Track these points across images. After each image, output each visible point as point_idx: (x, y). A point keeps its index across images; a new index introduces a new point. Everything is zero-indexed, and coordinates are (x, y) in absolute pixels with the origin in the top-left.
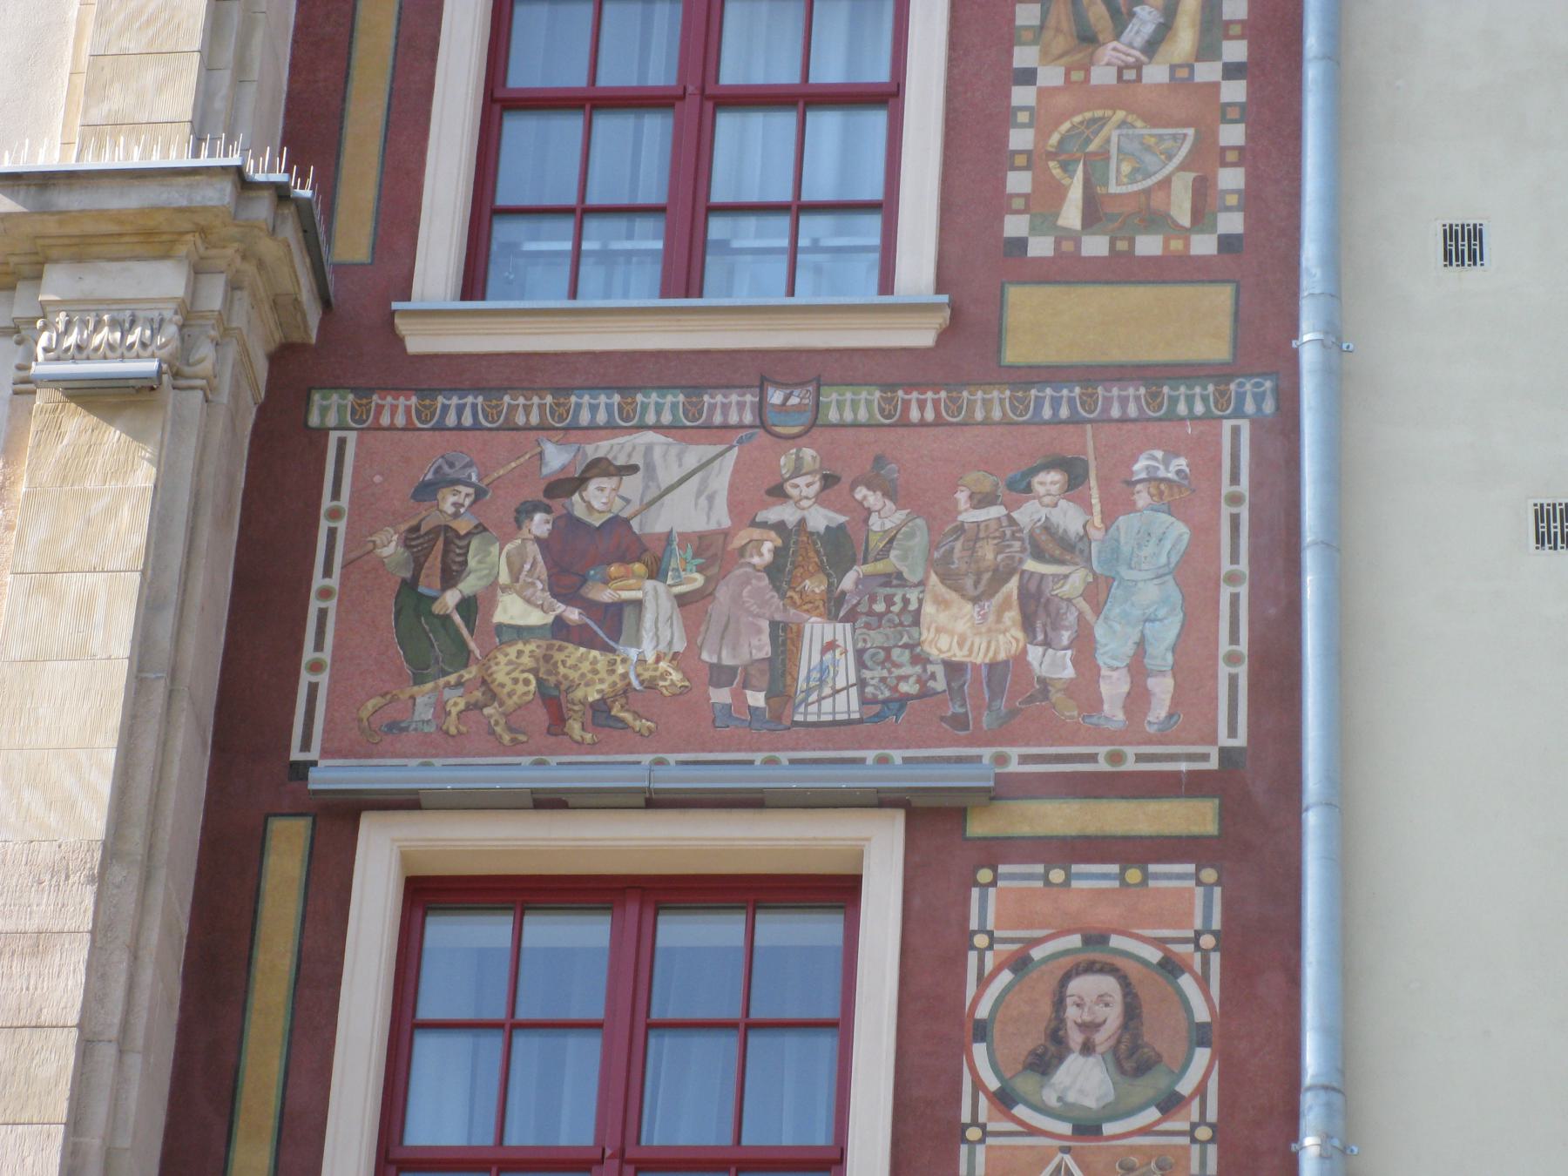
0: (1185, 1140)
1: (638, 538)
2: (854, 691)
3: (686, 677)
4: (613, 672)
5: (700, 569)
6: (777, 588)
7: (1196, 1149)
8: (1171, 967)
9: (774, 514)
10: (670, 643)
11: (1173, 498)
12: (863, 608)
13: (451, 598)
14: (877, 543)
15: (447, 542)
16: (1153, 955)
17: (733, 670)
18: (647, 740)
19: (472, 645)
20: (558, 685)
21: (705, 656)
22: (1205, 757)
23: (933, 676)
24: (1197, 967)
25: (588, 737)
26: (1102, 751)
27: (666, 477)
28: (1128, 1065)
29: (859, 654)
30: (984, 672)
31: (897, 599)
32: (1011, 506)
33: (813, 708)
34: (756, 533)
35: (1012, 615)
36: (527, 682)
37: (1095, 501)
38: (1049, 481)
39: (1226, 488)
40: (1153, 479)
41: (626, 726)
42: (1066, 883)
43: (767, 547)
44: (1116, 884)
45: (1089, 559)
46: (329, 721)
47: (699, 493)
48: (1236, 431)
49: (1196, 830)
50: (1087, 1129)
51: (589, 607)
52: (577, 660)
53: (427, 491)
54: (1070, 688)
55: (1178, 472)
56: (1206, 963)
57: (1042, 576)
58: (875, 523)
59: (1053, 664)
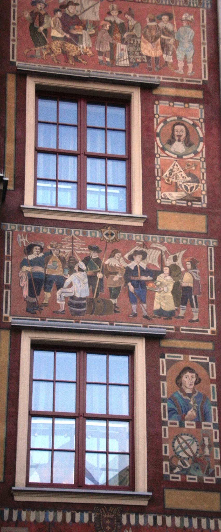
0: (199, 161)
1: (80, 21)
2: (128, 60)
3: (93, 52)
4: (77, 50)
5: (94, 29)
6: (111, 36)
7: (201, 163)
8: (195, 125)
9: (109, 18)
10: (89, 45)
11: (191, 24)
12: (128, 42)
13: (41, 29)
14: (131, 28)
15: (40, 16)
16: (191, 122)
17: (103, 53)
18: (86, 66)
19: (47, 40)
20: (66, 51)
21: (96, 49)
22: (200, 82)
23: (144, 59)
24: (200, 126)
25: (73, 64)
26: (179, 78)
27: (86, 7)
28: (187, 144)
29: (129, 52)
30: (154, 59)
31: (136, 41)
32: (158, 23)
33: (120, 63)
34: (105, 22)
35: (159, 47)
36: (59, 50)
37: (175, 23)
38: (165, 18)
39: (201, 24)
40: (186, 20)
41: (81, 62)
42: (173, 106)
43: (108, 26)
44: (183, 107)
45: (174, 37)
46: (17, 53)
47: (92, 12)
48: (203, 11)
49: (198, 97)
50: (180, 157)
51: (71, 35)
52: (70, 46)
53: (34, 4)
54: (172, 64)
55: (192, 19)
56: (201, 125)
57: (165, 39)
58: (130, 23)
59: (168, 58)
